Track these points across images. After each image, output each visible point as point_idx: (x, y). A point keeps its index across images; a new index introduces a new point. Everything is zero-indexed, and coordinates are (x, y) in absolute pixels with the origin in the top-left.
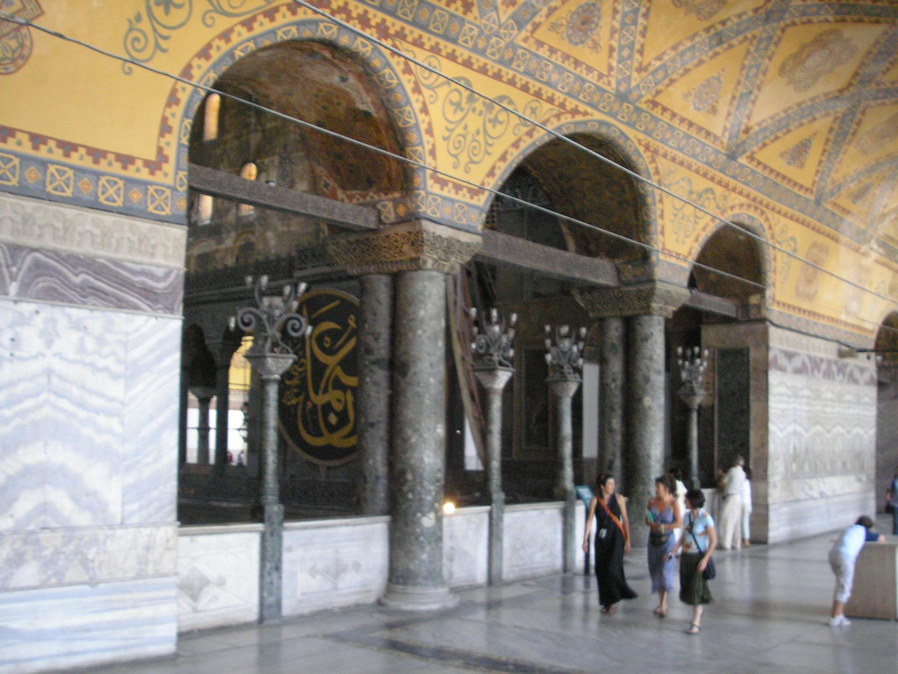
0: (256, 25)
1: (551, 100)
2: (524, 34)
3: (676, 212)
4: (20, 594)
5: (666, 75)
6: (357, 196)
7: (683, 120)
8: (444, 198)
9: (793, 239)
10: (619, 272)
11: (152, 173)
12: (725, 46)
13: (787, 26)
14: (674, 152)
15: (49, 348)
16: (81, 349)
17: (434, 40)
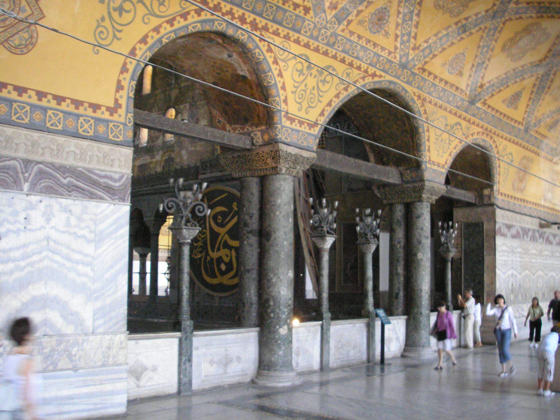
0: (175, 23)
1: (359, 68)
2: (342, 27)
3: (437, 138)
5: (431, 52)
6: (239, 128)
7: (441, 80)
8: (293, 130)
10: (402, 175)
11: (111, 115)
12: (468, 33)
13: (507, 21)
14: (436, 100)
15: (48, 223)
16: (68, 224)
17: (286, 31)
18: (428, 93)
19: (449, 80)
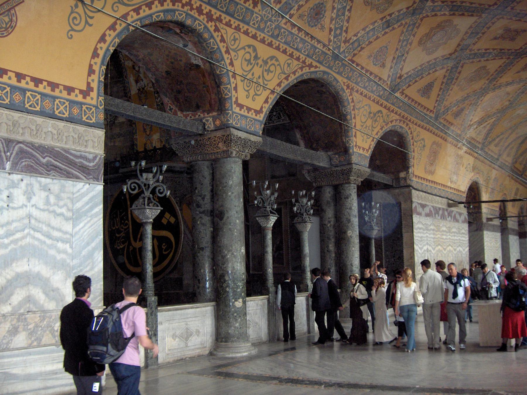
0: (141, 11)
1: (298, 59)
3: (362, 124)
4: (17, 352)
5: (359, 45)
6: (191, 115)
7: (367, 71)
8: (242, 116)
9: (423, 139)
10: (331, 159)
11: (84, 98)
12: (391, 28)
13: (424, 17)
14: (362, 90)
15: (29, 202)
16: (47, 202)
17: (237, 23)
18: (355, 83)
19: (373, 71)
